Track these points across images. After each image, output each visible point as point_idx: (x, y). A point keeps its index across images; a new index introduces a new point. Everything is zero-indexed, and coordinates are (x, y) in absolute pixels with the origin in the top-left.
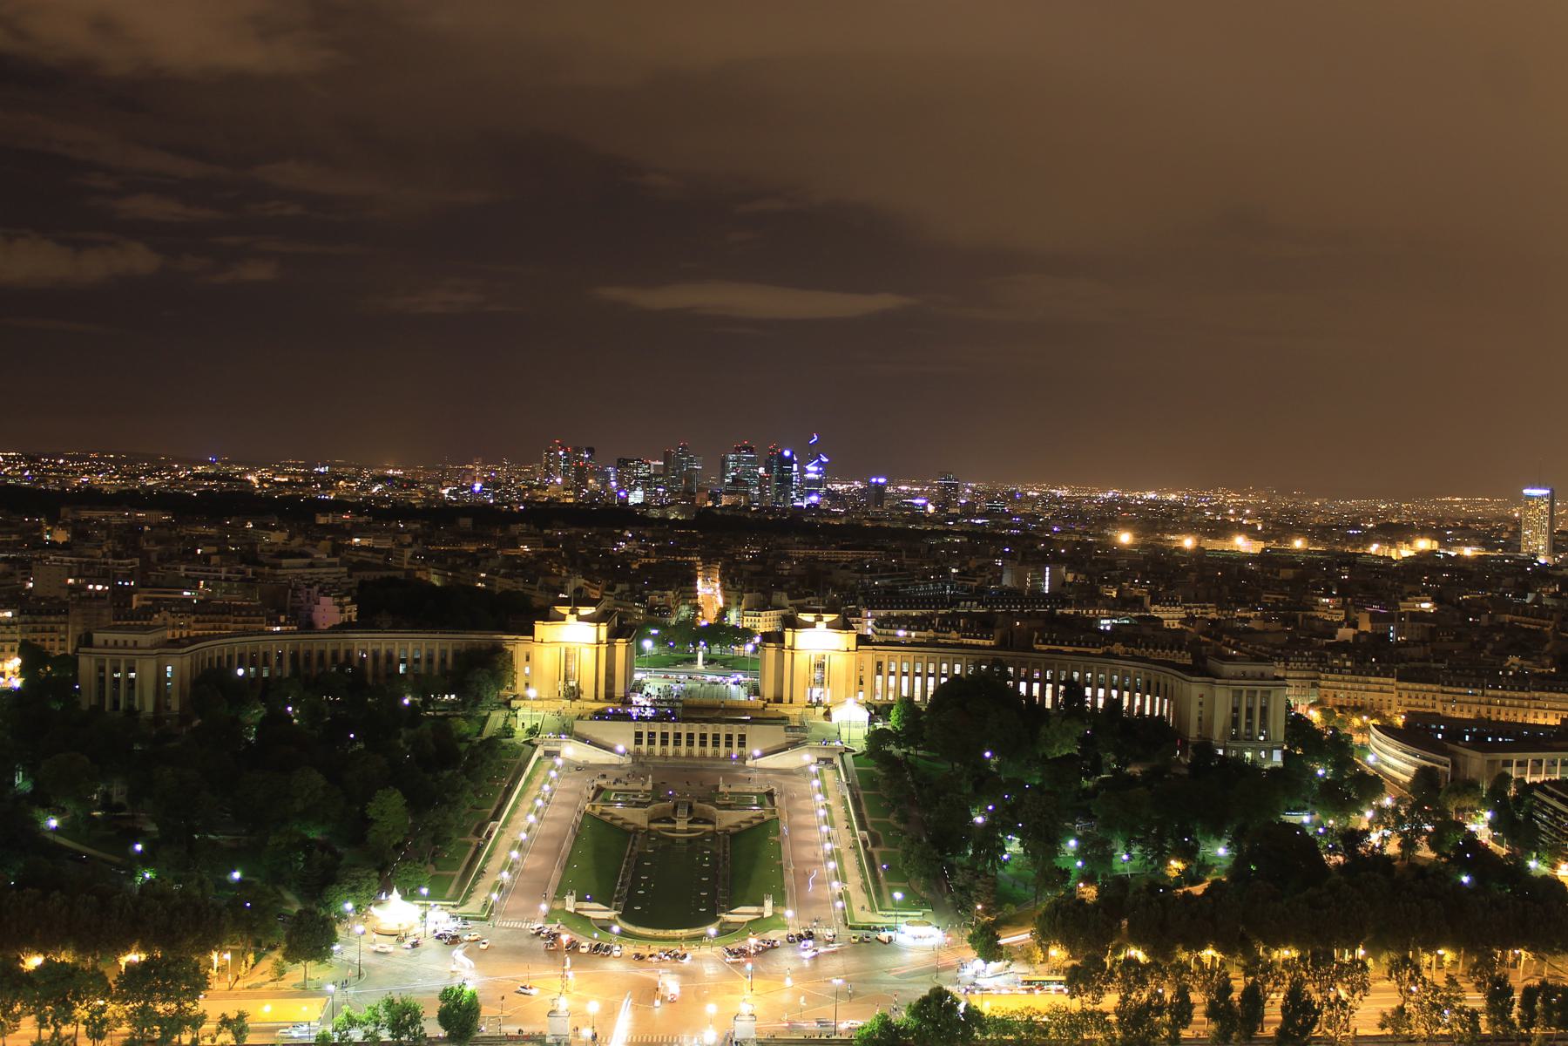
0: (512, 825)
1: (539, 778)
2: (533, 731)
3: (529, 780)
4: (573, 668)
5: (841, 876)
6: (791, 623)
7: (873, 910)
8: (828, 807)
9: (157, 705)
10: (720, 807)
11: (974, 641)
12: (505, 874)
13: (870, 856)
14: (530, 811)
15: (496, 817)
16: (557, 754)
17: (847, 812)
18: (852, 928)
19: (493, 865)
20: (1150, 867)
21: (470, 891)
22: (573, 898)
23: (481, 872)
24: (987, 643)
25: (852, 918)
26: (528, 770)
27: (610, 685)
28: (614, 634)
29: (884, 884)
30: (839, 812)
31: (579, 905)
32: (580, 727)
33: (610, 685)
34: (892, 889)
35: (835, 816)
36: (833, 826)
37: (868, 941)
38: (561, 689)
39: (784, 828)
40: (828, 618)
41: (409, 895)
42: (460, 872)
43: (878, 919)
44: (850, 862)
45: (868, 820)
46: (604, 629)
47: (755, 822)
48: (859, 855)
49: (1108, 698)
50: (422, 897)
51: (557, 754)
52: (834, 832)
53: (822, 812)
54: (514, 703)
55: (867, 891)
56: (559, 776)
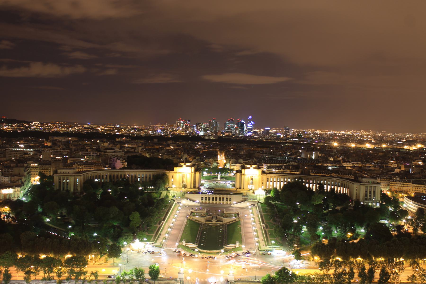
1: (176, 209)
2: (174, 197)
3: (173, 210)
4: (185, 180)
6: (244, 167)
7: (266, 246)
8: (254, 218)
9: (74, 189)
11: (294, 173)
13: (265, 231)
14: (173, 218)
15: (164, 220)
16: (180, 203)
17: (259, 219)
18: (260, 251)
19: (163, 233)
20: (342, 235)
21: (157, 240)
22: (185, 241)
23: (160, 234)
24: (297, 173)
25: (260, 248)
27: (195, 184)
28: (196, 170)
29: (269, 239)
30: (257, 219)
33: (195, 184)
34: (271, 240)
36: (255, 222)
37: (264, 254)
38: (181, 185)
39: (242, 223)
40: (254, 166)
41: (141, 240)
42: (154, 235)
43: (267, 248)
44: (260, 233)
45: (265, 221)
46: (193, 169)
47: (234, 221)
48: (262, 231)
49: (331, 188)
51: (180, 203)
52: (255, 224)
54: (169, 189)
55: (265, 241)
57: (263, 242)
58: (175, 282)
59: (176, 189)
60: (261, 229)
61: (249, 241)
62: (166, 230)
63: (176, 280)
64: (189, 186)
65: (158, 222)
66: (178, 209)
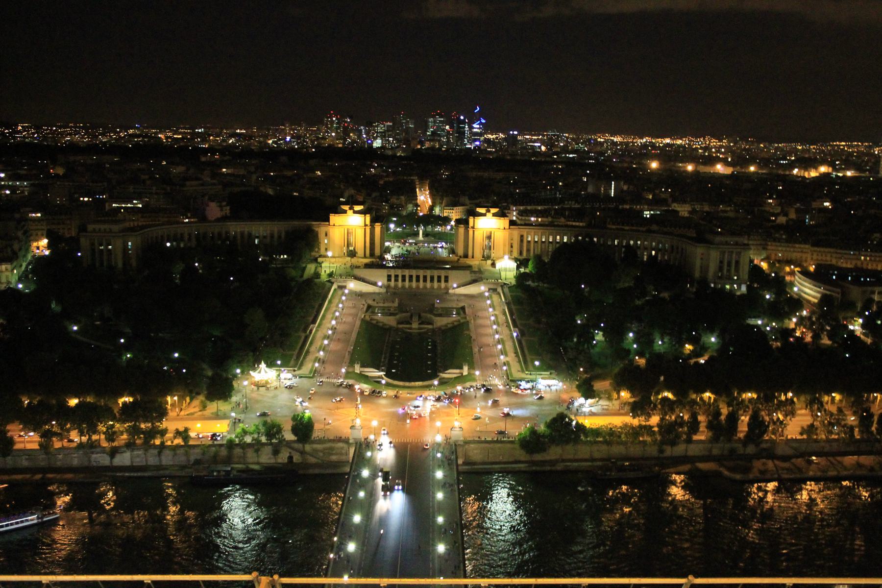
0: (322, 326)
1: (336, 301)
2: (331, 275)
3: (330, 302)
4: (352, 240)
5: (504, 352)
7: (523, 371)
8: (496, 316)
9: (124, 264)
11: (574, 224)
12: (322, 353)
14: (332, 319)
15: (314, 322)
23: (308, 352)
24: (581, 224)
25: (512, 376)
26: (330, 296)
28: (373, 221)
29: (528, 358)
30: (502, 319)
31: (362, 369)
32: (357, 272)
35: (499, 320)
36: (498, 325)
39: (471, 326)
40: (493, 210)
41: (270, 365)
42: (297, 351)
45: (518, 322)
46: (368, 217)
51: (345, 287)
52: (499, 329)
53: (493, 318)
54: (320, 260)
55: (519, 361)
56: (346, 299)
57: (518, 364)
58: (345, 446)
59: (333, 260)
61: (490, 361)
62: (319, 344)
63: (346, 441)
64: (360, 252)
65: (303, 327)
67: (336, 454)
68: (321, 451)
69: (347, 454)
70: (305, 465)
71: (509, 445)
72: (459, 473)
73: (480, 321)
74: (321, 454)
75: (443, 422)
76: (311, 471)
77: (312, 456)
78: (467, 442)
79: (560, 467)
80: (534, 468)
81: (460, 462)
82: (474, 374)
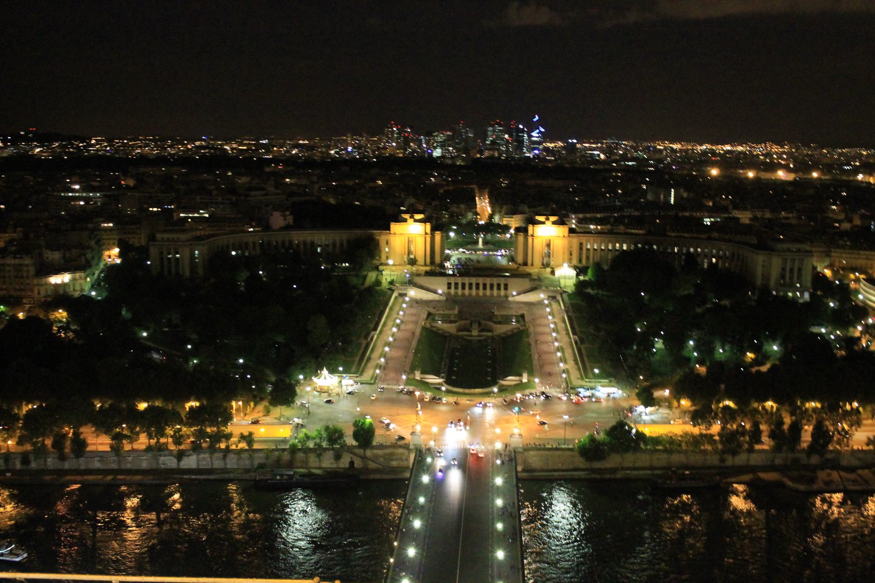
0: (383, 333)
1: (397, 308)
3: (391, 309)
4: (412, 249)
5: (563, 360)
7: (582, 378)
8: (555, 323)
10: (496, 323)
11: (633, 231)
12: (383, 360)
14: (393, 326)
15: (375, 329)
19: (375, 355)
23: (369, 359)
24: (641, 232)
25: (571, 383)
28: (433, 230)
29: (588, 365)
30: (561, 325)
31: (423, 376)
32: (418, 280)
36: (558, 332)
40: (553, 218)
41: (332, 371)
42: (357, 359)
44: (568, 353)
45: (578, 330)
46: (428, 226)
50: (339, 372)
51: (405, 295)
52: (559, 337)
53: (552, 326)
54: (381, 268)
55: (579, 369)
58: (405, 451)
59: (394, 268)
60: (572, 345)
61: (548, 369)
62: (380, 350)
64: (421, 260)
65: (364, 333)
66: (401, 306)
67: (397, 460)
68: (381, 457)
69: (407, 460)
70: (366, 470)
71: (568, 453)
72: (518, 480)
73: (541, 329)
74: (382, 460)
75: (502, 429)
76: (372, 477)
77: (373, 461)
78: (526, 449)
79: (619, 475)
80: (593, 476)
81: (519, 468)
82: (534, 382)
